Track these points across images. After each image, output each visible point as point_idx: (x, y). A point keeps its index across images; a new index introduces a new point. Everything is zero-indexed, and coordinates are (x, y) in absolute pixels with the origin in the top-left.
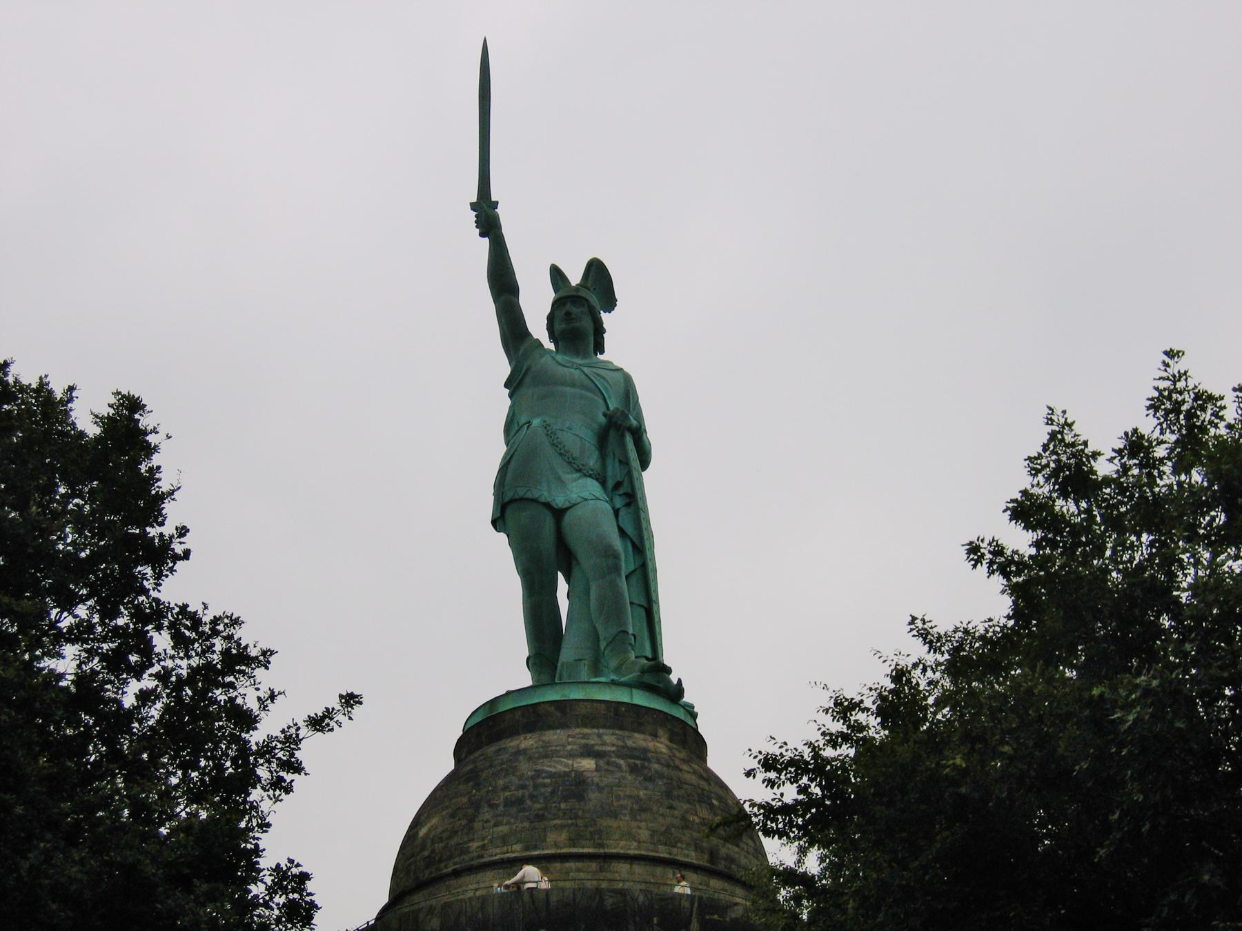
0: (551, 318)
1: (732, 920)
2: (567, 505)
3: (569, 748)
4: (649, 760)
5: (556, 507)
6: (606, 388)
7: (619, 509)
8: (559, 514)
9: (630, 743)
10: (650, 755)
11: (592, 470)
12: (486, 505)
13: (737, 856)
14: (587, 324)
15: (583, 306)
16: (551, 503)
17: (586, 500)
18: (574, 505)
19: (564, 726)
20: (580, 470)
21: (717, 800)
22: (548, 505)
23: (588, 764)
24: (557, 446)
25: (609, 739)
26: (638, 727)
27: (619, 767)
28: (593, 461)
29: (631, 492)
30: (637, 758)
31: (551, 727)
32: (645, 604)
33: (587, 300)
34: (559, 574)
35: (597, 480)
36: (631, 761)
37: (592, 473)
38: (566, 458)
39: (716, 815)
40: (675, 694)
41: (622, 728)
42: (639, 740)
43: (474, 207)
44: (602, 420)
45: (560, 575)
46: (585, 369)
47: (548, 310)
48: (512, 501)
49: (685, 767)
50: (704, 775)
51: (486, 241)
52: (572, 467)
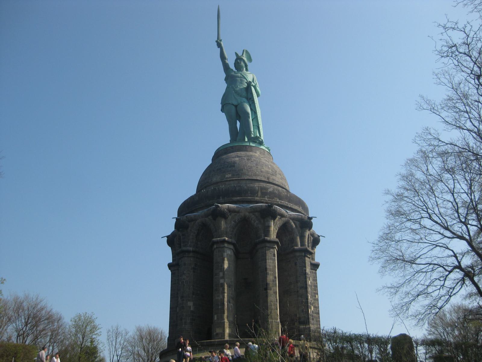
0: (235, 64)
1: (269, 191)
3: (233, 156)
4: (252, 157)
6: (247, 77)
8: (236, 106)
9: (248, 154)
10: (253, 156)
12: (220, 106)
13: (275, 179)
14: (242, 64)
19: (233, 152)
20: (241, 96)
21: (270, 166)
23: (237, 159)
25: (242, 153)
26: (251, 151)
27: (244, 159)
30: (249, 157)
31: (230, 153)
32: (257, 125)
33: (242, 59)
34: (237, 121)
35: (245, 98)
36: (248, 158)
39: (269, 169)
40: (261, 143)
41: (247, 151)
42: (251, 153)
43: (217, 41)
44: (246, 84)
45: (237, 121)
46: (242, 74)
47: (234, 62)
48: (224, 105)
49: (262, 159)
50: (268, 160)
51: (219, 49)
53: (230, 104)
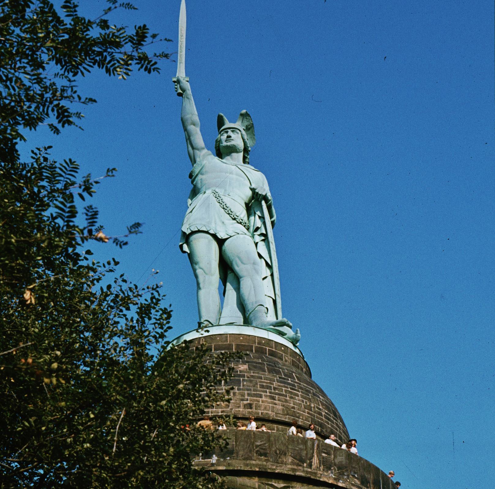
2: (227, 237)
5: (220, 238)
7: (257, 243)
8: (221, 242)
11: (242, 220)
15: (238, 133)
16: (217, 234)
17: (238, 234)
18: (231, 237)
20: (234, 219)
22: (214, 236)
24: (221, 204)
28: (242, 213)
29: (265, 232)
33: (240, 131)
35: (245, 226)
37: (242, 221)
38: (227, 211)
52: (230, 216)
53: (207, 232)
